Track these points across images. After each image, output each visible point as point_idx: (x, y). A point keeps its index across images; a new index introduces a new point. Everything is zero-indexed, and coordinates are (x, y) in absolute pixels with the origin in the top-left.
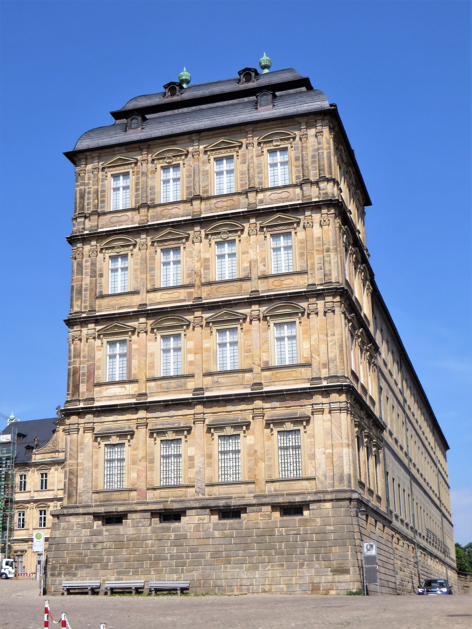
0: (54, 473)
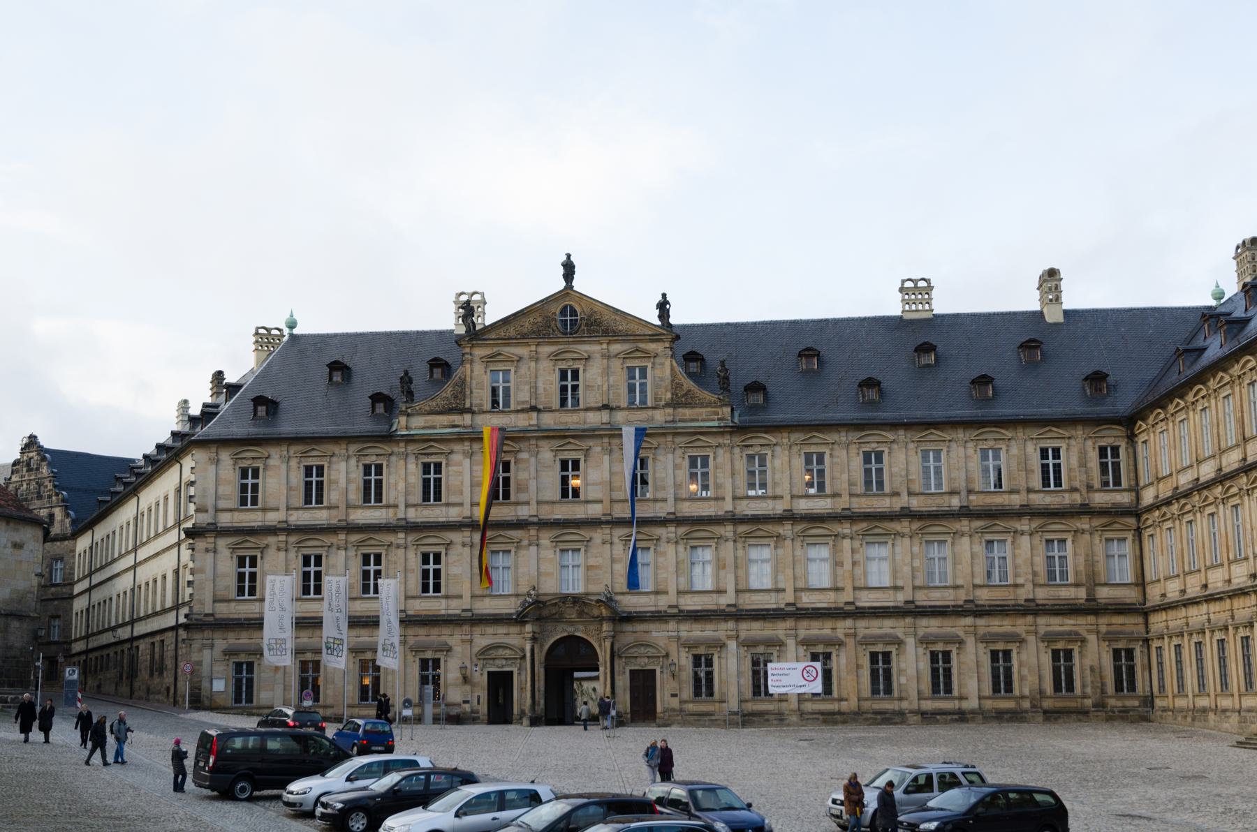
0: (460, 464)
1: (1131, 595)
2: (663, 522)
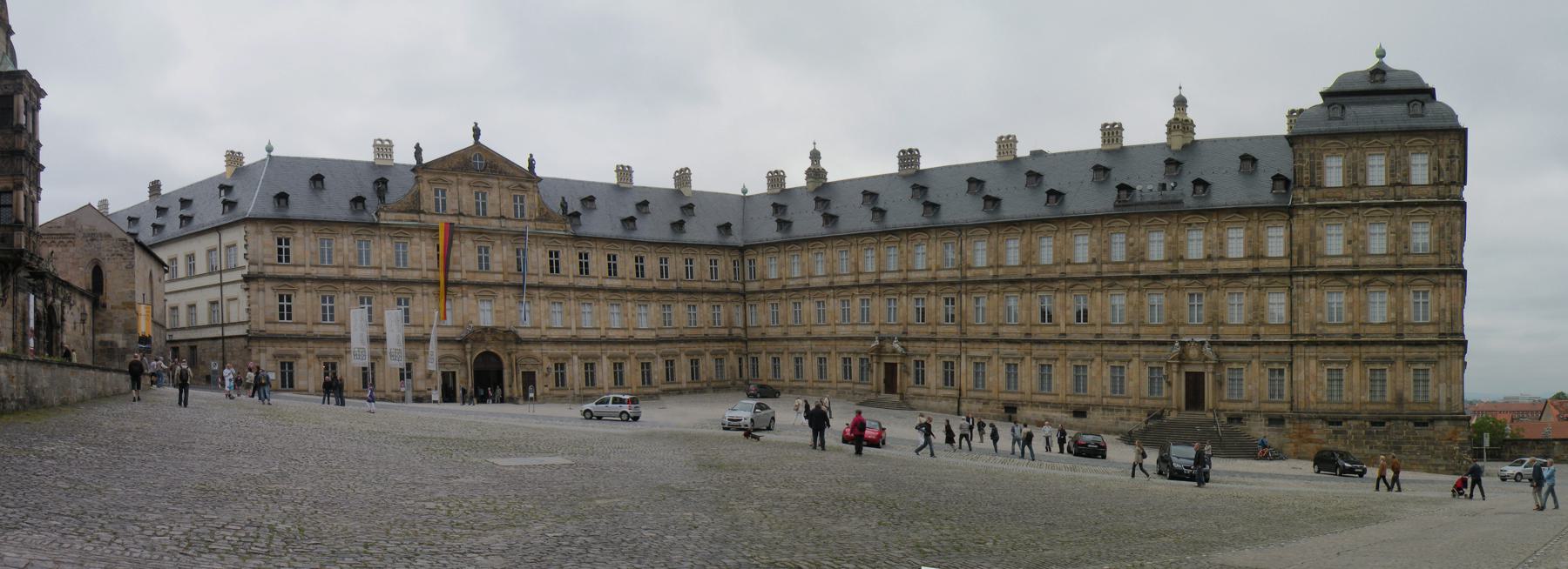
1: (741, 333)
2: (538, 287)
